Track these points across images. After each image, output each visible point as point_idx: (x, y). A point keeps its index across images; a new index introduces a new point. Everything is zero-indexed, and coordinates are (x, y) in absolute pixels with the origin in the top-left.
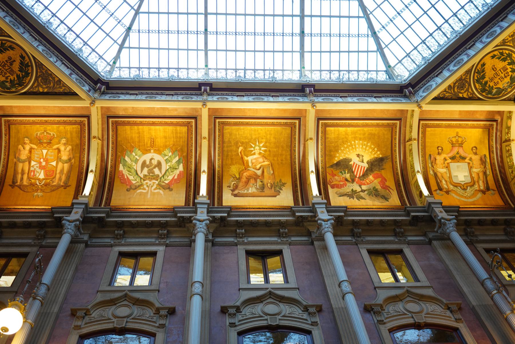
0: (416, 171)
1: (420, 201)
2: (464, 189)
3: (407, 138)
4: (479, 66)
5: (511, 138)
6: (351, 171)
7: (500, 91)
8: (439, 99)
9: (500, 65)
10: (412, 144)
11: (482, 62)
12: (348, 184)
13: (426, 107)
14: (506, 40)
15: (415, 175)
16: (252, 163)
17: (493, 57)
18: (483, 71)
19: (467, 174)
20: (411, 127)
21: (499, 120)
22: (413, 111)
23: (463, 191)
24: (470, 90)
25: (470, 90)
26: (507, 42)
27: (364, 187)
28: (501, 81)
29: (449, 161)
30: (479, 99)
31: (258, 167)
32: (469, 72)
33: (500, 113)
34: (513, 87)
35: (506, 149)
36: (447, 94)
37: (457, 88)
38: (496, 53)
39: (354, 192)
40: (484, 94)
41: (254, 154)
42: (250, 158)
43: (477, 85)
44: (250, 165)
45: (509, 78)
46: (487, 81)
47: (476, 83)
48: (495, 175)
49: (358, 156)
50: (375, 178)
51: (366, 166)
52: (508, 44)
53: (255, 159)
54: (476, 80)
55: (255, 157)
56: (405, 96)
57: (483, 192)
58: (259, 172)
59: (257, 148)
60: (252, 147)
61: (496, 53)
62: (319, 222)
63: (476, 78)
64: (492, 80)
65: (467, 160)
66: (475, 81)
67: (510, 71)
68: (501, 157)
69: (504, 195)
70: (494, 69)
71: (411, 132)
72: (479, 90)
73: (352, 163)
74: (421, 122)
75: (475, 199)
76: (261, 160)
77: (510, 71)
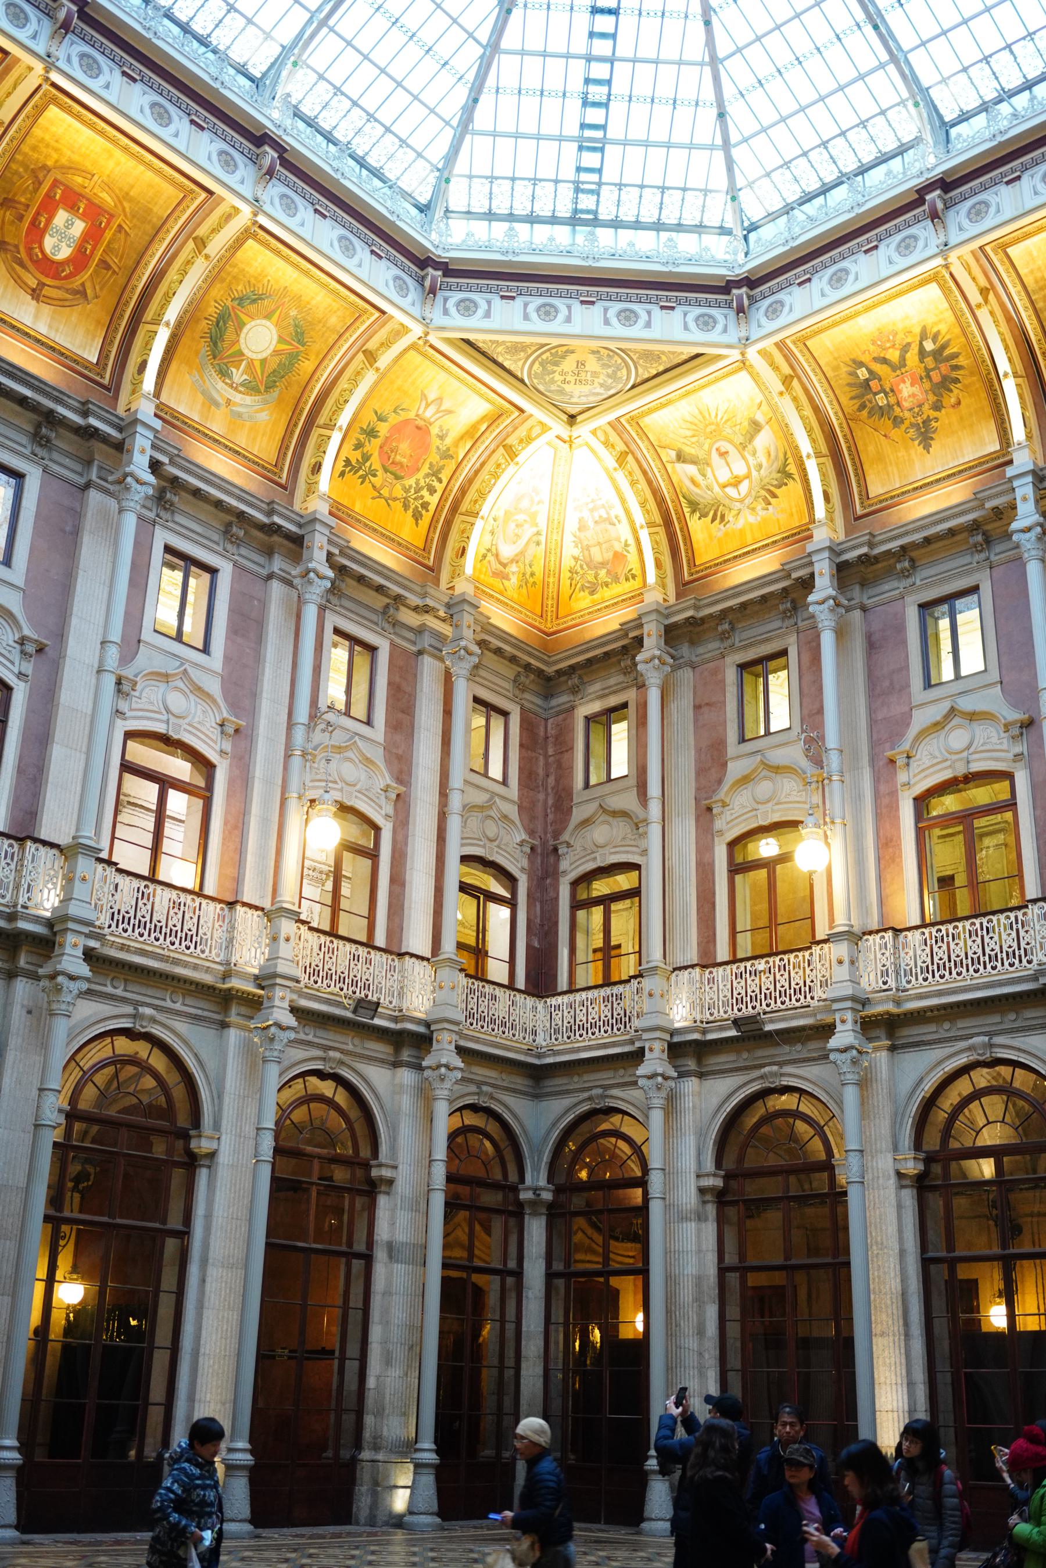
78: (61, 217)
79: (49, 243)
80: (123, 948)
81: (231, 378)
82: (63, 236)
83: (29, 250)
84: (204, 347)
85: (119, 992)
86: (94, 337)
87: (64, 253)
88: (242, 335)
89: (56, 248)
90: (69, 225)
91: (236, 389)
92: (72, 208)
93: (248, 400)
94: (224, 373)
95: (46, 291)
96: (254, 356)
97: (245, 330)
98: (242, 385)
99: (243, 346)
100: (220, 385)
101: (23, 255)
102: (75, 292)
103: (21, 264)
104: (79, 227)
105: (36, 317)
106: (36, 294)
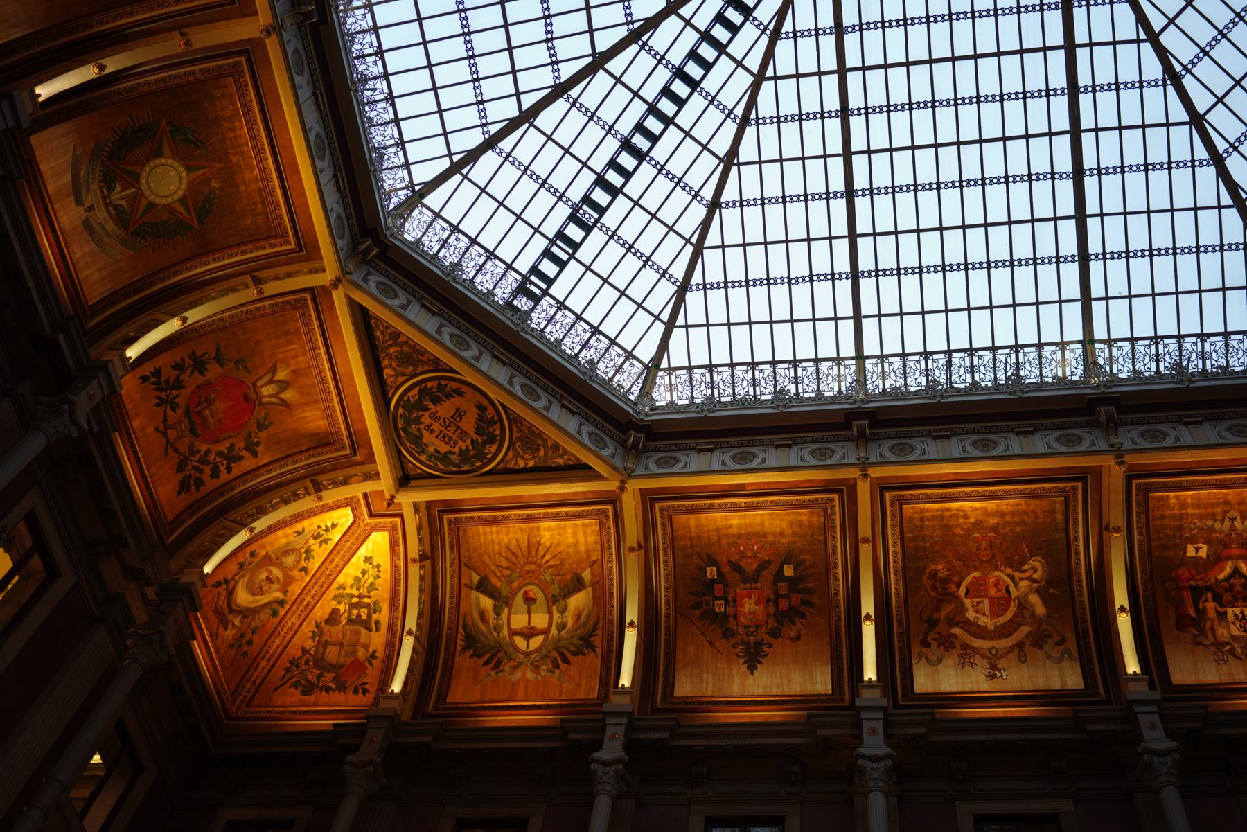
0: (186, 314)
1: (114, 344)
3: (262, 274)
4: (455, 385)
5: (323, 494)
7: (417, 440)
8: (363, 319)
9: (469, 424)
10: (248, 288)
11: (464, 389)
13: (338, 297)
14: (521, 423)
15: (173, 316)
17: (481, 408)
18: (448, 396)
20: (289, 275)
21: (358, 458)
22: (324, 270)
24: (401, 379)
25: (401, 379)
26: (517, 427)
28: (437, 437)
30: (388, 403)
32: (437, 365)
33: (371, 458)
34: (429, 463)
35: (298, 490)
36: (378, 334)
37: (397, 351)
38: (491, 410)
40: (401, 410)
43: (414, 392)
45: (447, 448)
46: (430, 409)
47: (418, 388)
48: (233, 484)
52: (515, 429)
54: (426, 386)
56: (354, 245)
61: (491, 410)
63: (429, 385)
64: (434, 417)
66: (423, 385)
67: (460, 449)
68: (279, 485)
69: (193, 513)
70: (459, 413)
71: (276, 279)
72: (405, 398)
74: (307, 296)
77: (460, 449)
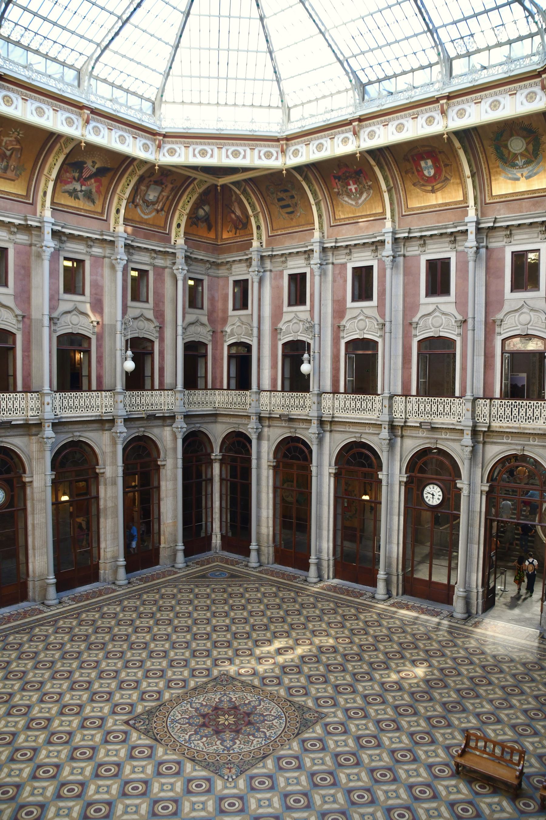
2: (148, 206)
6: (81, 173)
12: (74, 182)
16: (6, 143)
19: (157, 195)
23: (145, 207)
27: (84, 188)
29: (152, 183)
31: (10, 148)
39: (75, 190)
41: (11, 137)
42: (5, 139)
44: (3, 144)
49: (93, 162)
50: (95, 182)
51: (94, 170)
53: (10, 141)
55: (11, 139)
57: (158, 211)
58: (8, 153)
59: (16, 133)
60: (11, 131)
62: (44, 248)
65: (163, 186)
73: (85, 166)
75: (149, 216)
76: (14, 143)
78: (423, 164)
79: (426, 173)
80: (500, 427)
81: (517, 165)
82: (428, 168)
83: (423, 179)
84: (499, 163)
85: (509, 441)
86: (458, 190)
87: (432, 172)
88: (510, 148)
89: (429, 172)
90: (426, 163)
91: (523, 168)
92: (423, 159)
93: (530, 168)
94: (514, 166)
95: (436, 187)
96: (521, 151)
97: (509, 146)
98: (524, 164)
99: (514, 151)
100: (515, 171)
101: (422, 182)
102: (444, 181)
103: (424, 185)
104: (430, 162)
105: (436, 198)
106: (433, 191)
